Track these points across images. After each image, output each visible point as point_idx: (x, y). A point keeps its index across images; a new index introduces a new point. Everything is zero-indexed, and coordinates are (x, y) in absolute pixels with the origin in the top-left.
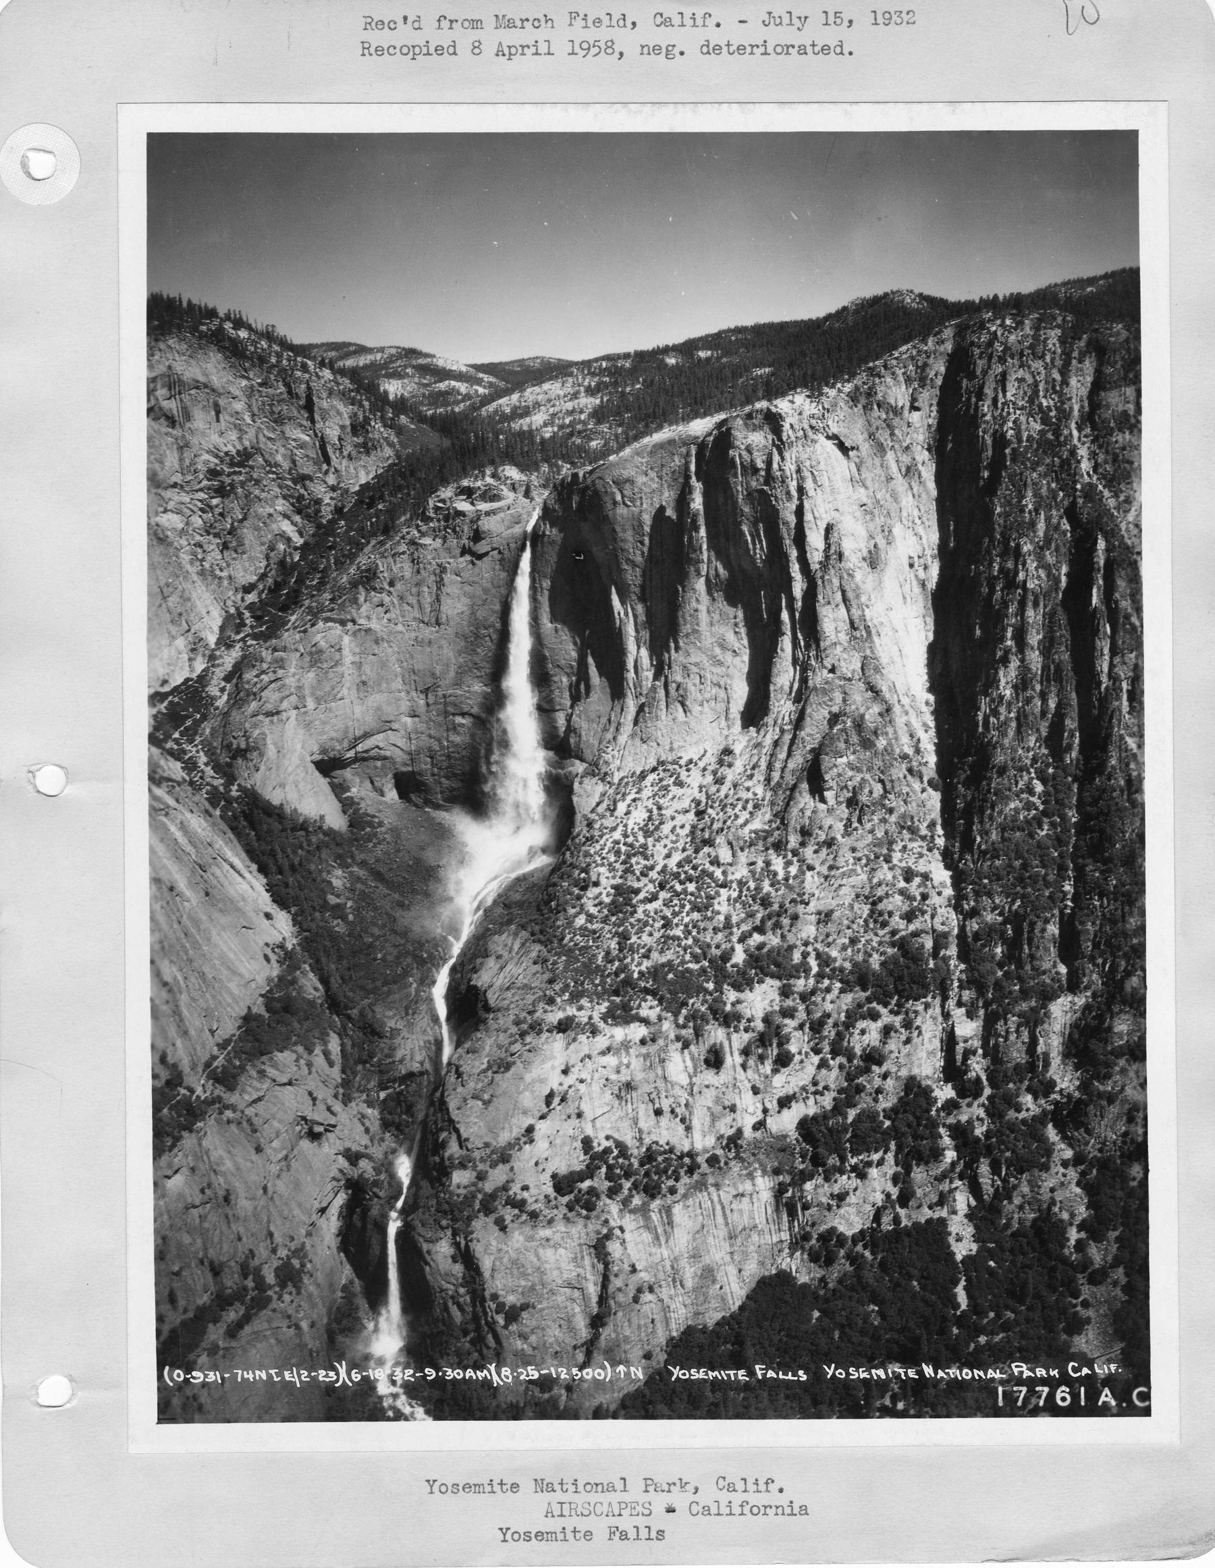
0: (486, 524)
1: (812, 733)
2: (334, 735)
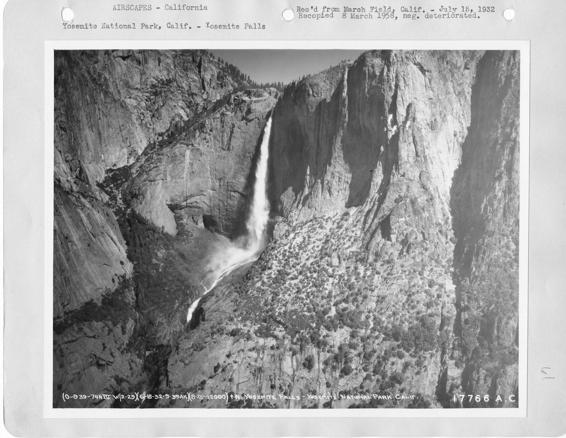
0: (253, 106)
1: (388, 203)
2: (177, 193)
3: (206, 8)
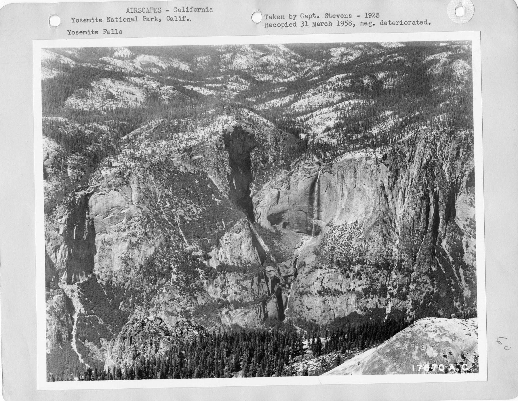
3: (211, 10)
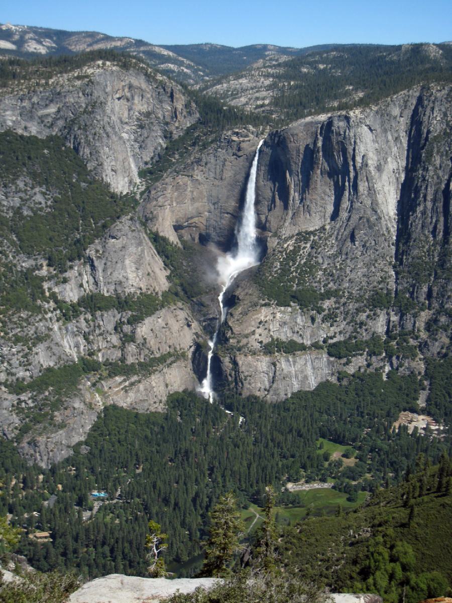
0: (243, 145)
1: (352, 223)
